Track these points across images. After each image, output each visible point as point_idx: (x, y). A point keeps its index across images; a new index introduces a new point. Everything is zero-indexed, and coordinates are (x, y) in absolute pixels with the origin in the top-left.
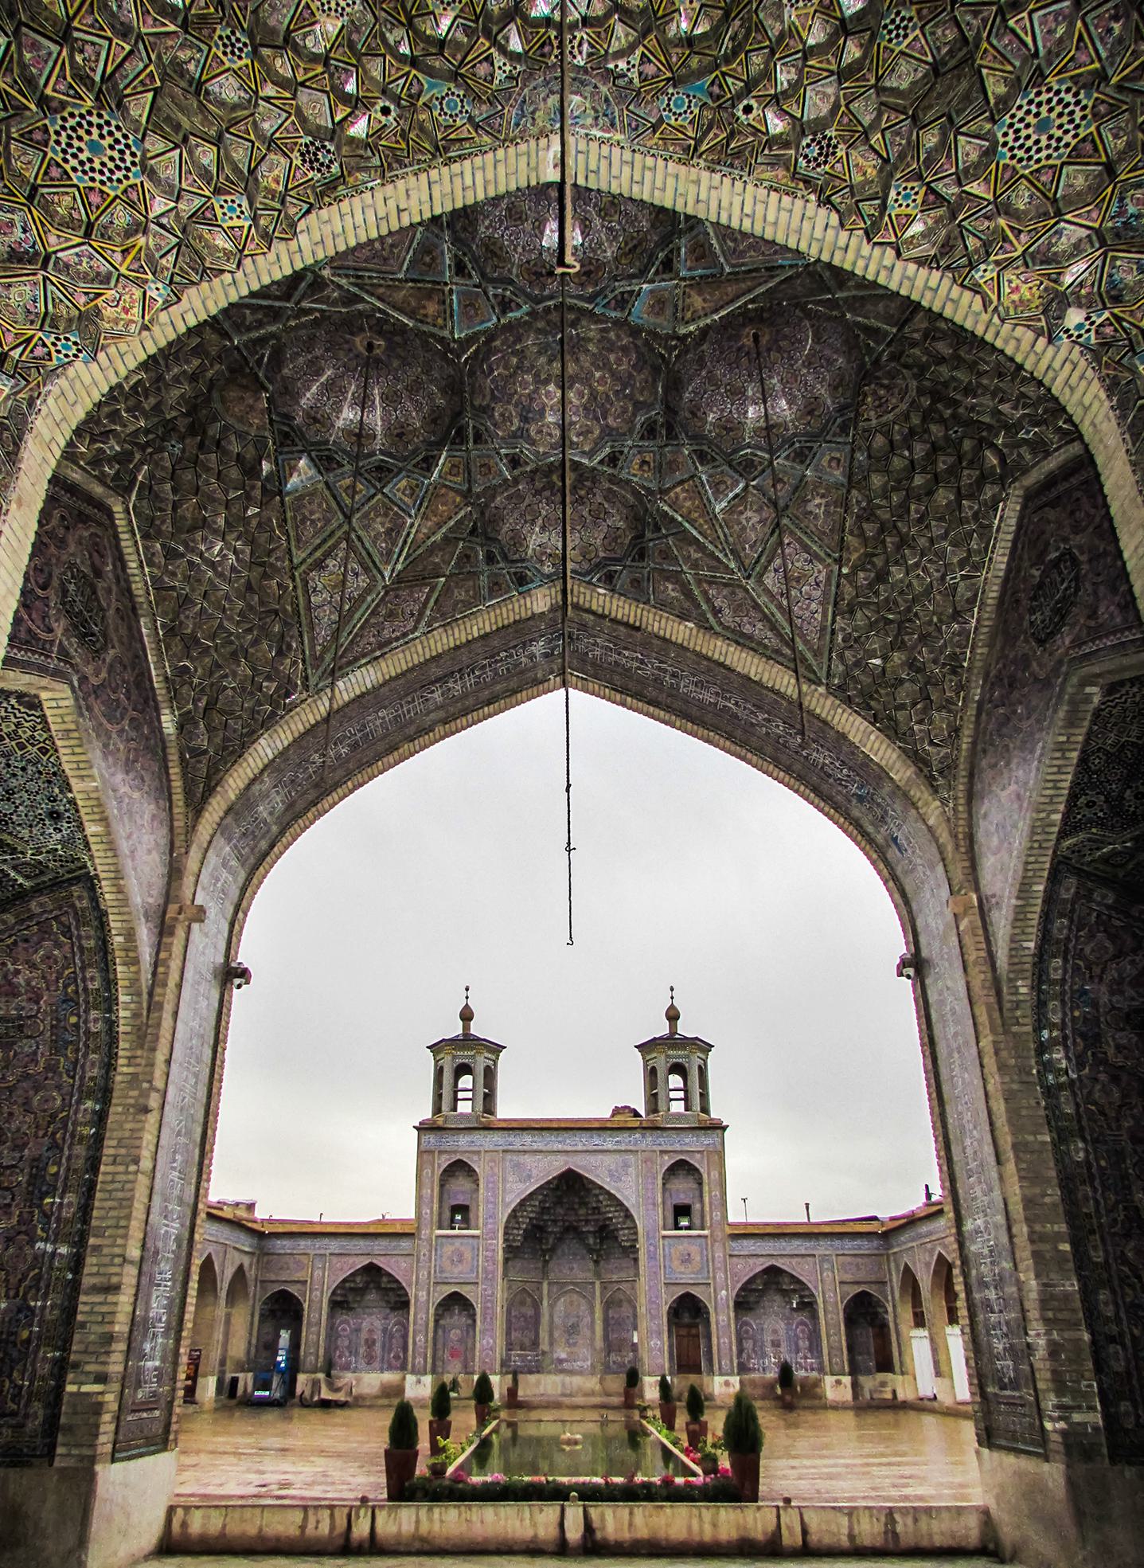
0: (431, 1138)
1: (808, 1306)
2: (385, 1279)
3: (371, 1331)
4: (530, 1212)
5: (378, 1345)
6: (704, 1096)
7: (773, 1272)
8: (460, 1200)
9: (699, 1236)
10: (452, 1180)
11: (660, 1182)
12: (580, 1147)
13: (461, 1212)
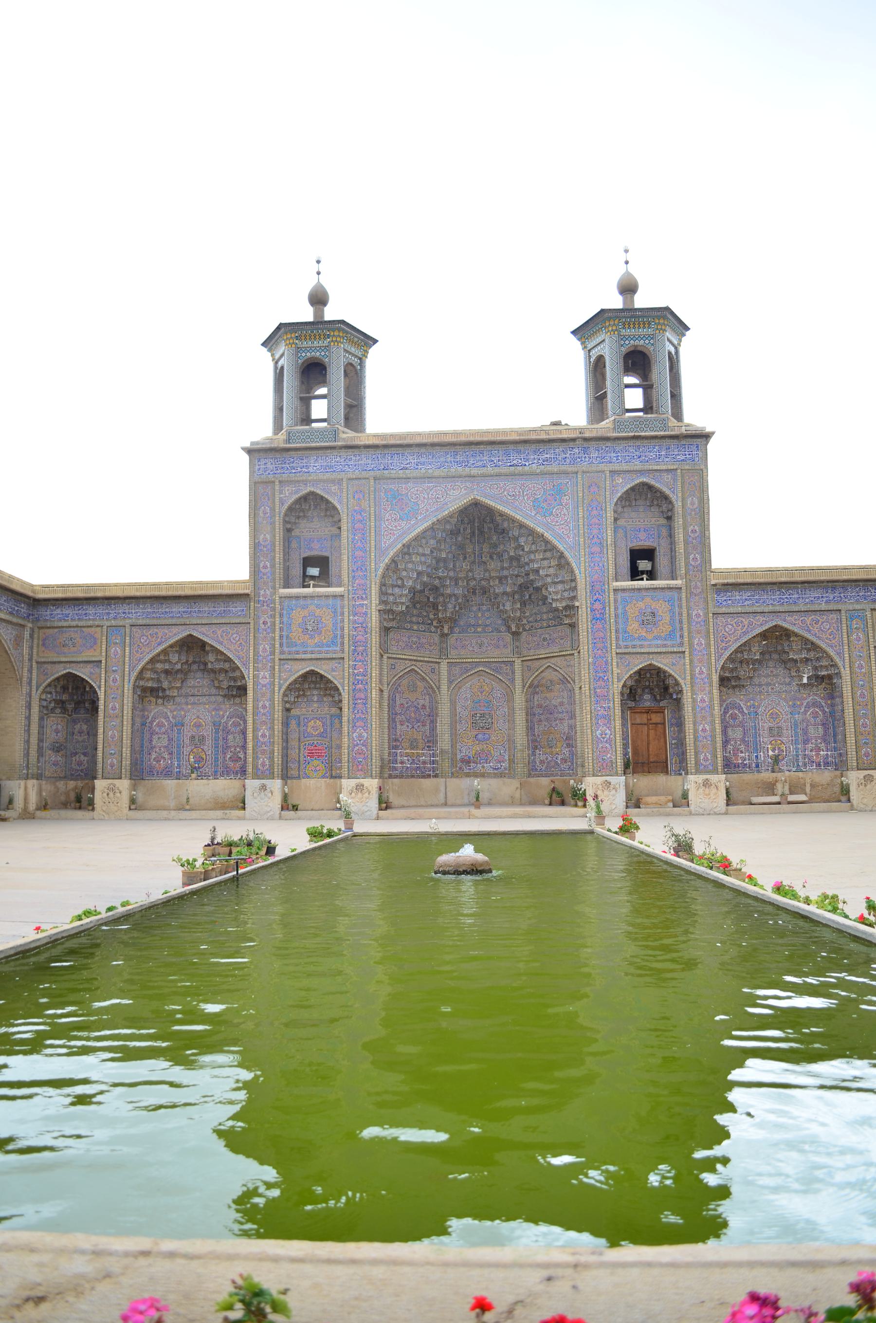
2: (211, 657)
4: (419, 563)
5: (209, 742)
6: (676, 397)
8: (316, 551)
9: (670, 588)
10: (303, 523)
11: (610, 514)
12: (490, 470)
13: (318, 567)
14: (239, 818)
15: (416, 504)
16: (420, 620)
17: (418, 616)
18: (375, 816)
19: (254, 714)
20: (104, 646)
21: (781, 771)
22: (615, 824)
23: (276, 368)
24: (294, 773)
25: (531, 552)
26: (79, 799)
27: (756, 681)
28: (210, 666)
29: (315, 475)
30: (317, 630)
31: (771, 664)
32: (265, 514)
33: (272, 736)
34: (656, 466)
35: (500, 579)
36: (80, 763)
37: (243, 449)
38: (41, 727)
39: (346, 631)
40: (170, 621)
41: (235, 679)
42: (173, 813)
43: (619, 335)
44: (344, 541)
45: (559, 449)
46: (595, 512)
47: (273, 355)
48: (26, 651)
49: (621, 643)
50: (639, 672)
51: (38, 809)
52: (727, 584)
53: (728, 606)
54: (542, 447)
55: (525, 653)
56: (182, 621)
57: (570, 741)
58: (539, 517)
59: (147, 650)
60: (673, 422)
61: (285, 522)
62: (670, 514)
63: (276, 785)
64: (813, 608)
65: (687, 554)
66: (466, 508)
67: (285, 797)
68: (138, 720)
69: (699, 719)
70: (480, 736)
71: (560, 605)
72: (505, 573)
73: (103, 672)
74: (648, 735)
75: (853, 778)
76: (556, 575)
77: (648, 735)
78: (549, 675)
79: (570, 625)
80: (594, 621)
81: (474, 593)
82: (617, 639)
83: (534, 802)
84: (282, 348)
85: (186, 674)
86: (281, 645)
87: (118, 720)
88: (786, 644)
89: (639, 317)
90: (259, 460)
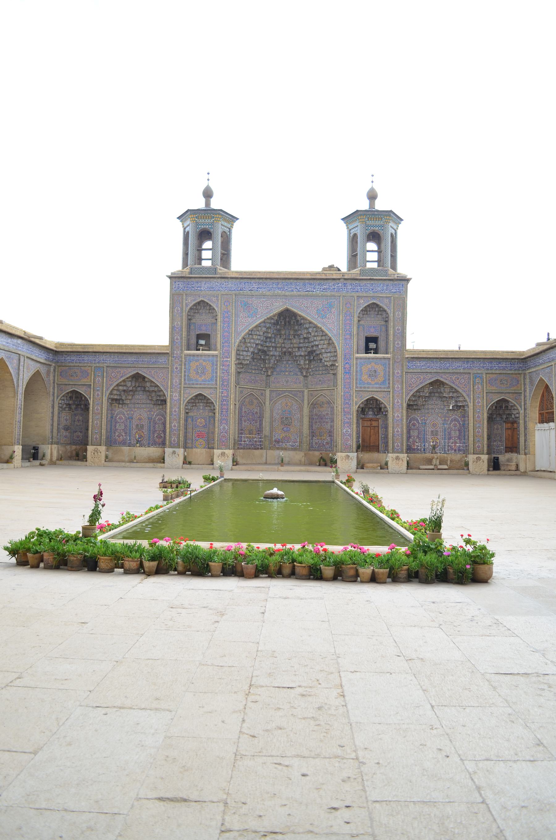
0: (181, 284)
1: (460, 408)
2: (148, 384)
3: (140, 419)
4: (257, 339)
5: (146, 428)
7: (437, 384)
9: (384, 358)
10: (197, 316)
11: (356, 319)
12: (295, 293)
13: (203, 340)
14: (161, 468)
15: (256, 309)
16: (256, 368)
17: (255, 366)
18: (230, 469)
19: (171, 415)
20: (93, 377)
21: (436, 453)
22: (344, 478)
23: (184, 231)
24: (190, 445)
25: (315, 336)
26: (77, 455)
27: (426, 407)
28: (147, 389)
29: (204, 291)
30: (203, 373)
31: (434, 398)
32: (178, 311)
33: (179, 426)
34: (380, 294)
35: (299, 348)
36: (78, 437)
37: (167, 276)
38: (59, 417)
39: (218, 374)
40: (127, 365)
41: (160, 396)
42: (128, 464)
43: (366, 224)
44: (219, 327)
45: (331, 283)
46: (348, 317)
47: (183, 224)
48: (51, 378)
49: (358, 385)
50: (367, 400)
51: (57, 460)
52: (414, 358)
53: (413, 369)
54: (322, 282)
55: (310, 386)
56: (134, 365)
57: (331, 433)
58: (319, 319)
59: (115, 380)
60: (391, 271)
61: (188, 315)
62: (387, 319)
63: (181, 451)
64: (456, 371)
65: (394, 341)
66: (282, 312)
67: (185, 458)
68: (109, 415)
69: (395, 426)
70: (285, 429)
71: (329, 364)
72: (301, 345)
73: (92, 391)
74: (370, 432)
75: (471, 458)
76: (327, 348)
77: (370, 432)
78: (322, 399)
79: (333, 374)
81: (285, 354)
82: (356, 383)
83: (311, 464)
84: (188, 222)
85: (134, 393)
86: (185, 380)
87: (100, 416)
88: (442, 389)
89: (376, 215)
90: (175, 282)
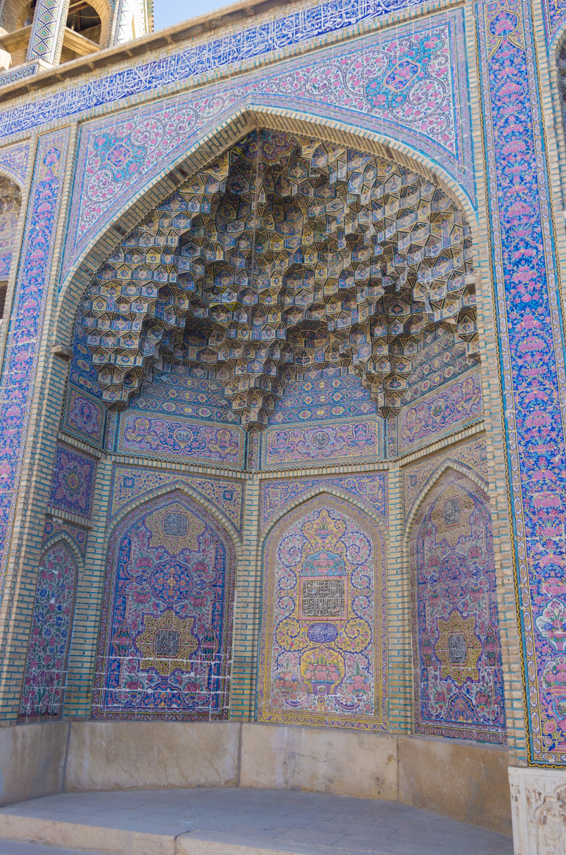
72: (349, 282)
80: (515, 314)
